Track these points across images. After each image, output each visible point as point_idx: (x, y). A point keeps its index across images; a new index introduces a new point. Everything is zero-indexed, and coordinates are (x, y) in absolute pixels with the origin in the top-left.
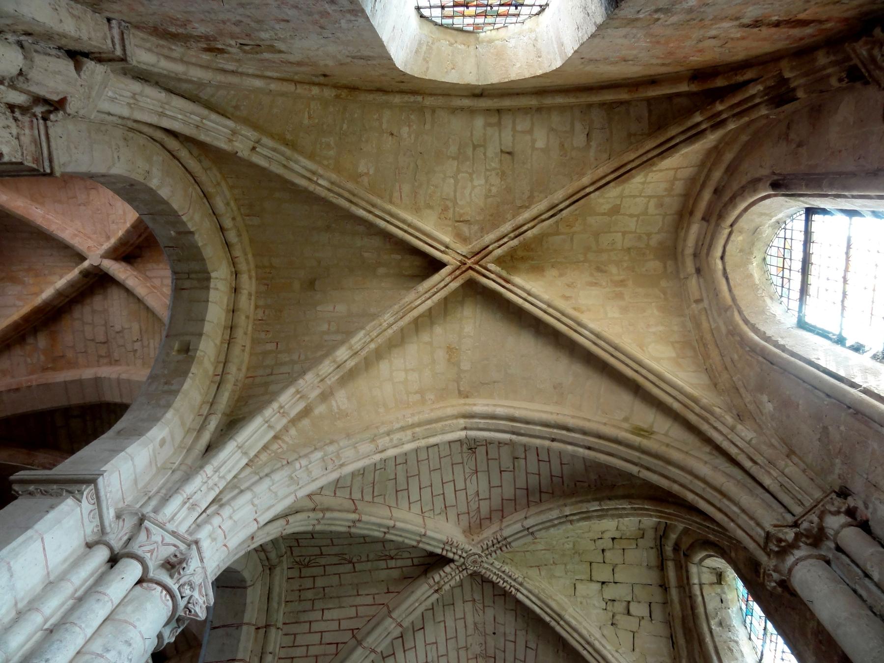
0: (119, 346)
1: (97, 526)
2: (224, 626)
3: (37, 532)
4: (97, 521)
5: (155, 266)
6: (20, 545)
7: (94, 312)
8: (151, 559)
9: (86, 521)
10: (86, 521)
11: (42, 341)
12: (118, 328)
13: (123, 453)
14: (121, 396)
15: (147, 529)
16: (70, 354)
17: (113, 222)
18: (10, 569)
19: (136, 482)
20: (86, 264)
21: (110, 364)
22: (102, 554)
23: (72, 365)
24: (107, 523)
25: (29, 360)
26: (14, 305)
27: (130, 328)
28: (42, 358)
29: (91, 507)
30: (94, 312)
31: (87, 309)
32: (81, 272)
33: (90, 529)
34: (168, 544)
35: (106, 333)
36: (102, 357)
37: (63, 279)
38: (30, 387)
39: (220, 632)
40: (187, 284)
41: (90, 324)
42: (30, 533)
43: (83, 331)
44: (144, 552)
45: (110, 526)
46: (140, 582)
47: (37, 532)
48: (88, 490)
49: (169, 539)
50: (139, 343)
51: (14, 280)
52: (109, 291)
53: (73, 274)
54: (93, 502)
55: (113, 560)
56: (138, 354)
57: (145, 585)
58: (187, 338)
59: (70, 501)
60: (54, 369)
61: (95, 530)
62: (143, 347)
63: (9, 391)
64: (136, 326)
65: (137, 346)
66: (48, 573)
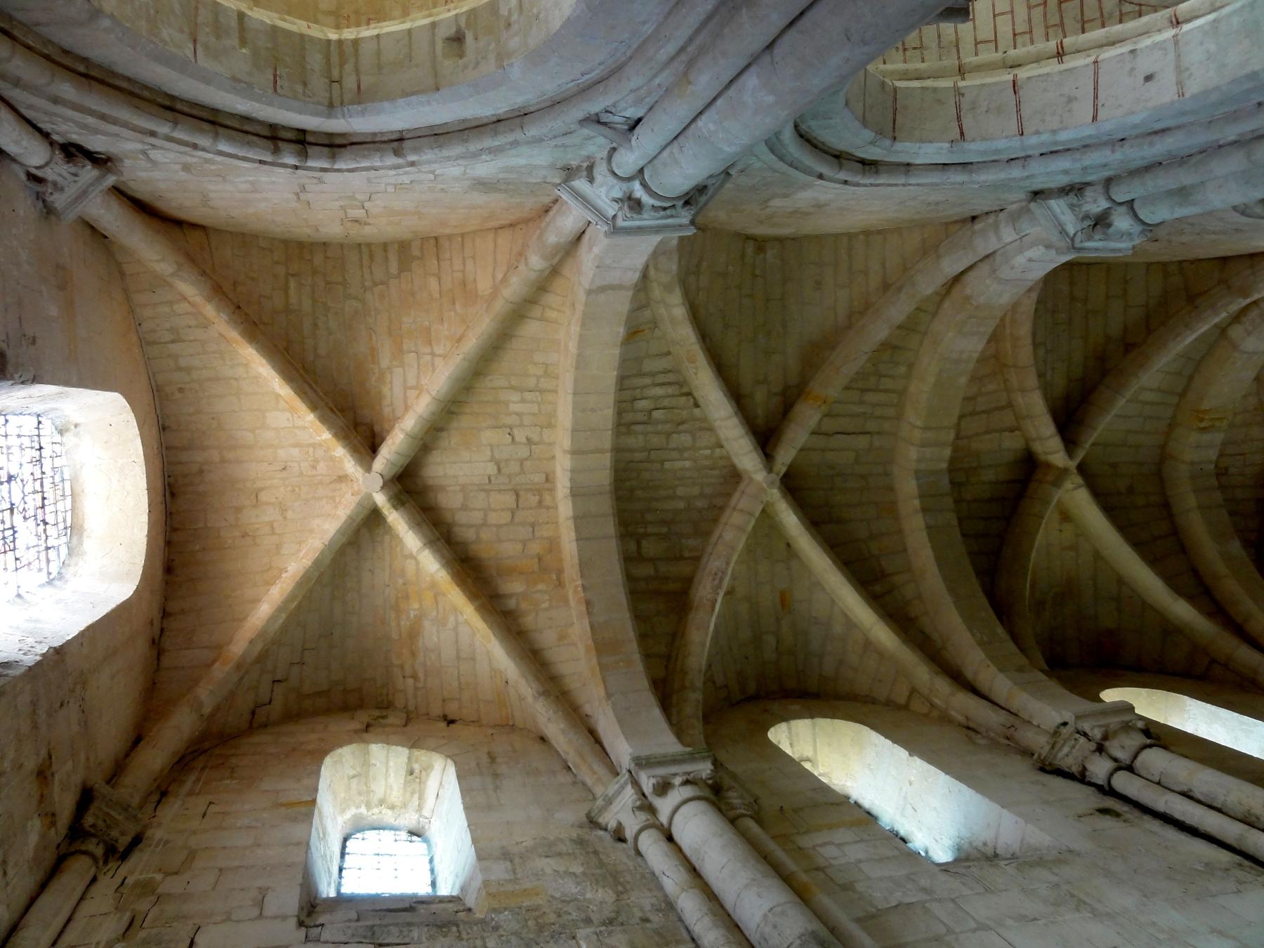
0: (522, 472)
2: (959, 118)
5: (386, 402)
7: (464, 508)
11: (513, 587)
12: (491, 469)
14: (601, 451)
16: (535, 548)
17: (314, 467)
20: (381, 499)
21: (552, 490)
23: (553, 545)
25: (543, 606)
26: (455, 629)
27: (491, 446)
28: (541, 587)
30: (464, 508)
31: (462, 518)
32: (395, 507)
35: (500, 491)
36: (540, 502)
37: (405, 532)
38: (583, 586)
39: (967, 122)
40: (350, 82)
41: (486, 516)
43: (499, 526)
50: (516, 432)
51: (414, 634)
52: (431, 482)
53: (396, 520)
56: (535, 438)
58: (439, 45)
60: (560, 572)
62: (521, 425)
63: (589, 613)
64: (488, 436)
65: (520, 436)
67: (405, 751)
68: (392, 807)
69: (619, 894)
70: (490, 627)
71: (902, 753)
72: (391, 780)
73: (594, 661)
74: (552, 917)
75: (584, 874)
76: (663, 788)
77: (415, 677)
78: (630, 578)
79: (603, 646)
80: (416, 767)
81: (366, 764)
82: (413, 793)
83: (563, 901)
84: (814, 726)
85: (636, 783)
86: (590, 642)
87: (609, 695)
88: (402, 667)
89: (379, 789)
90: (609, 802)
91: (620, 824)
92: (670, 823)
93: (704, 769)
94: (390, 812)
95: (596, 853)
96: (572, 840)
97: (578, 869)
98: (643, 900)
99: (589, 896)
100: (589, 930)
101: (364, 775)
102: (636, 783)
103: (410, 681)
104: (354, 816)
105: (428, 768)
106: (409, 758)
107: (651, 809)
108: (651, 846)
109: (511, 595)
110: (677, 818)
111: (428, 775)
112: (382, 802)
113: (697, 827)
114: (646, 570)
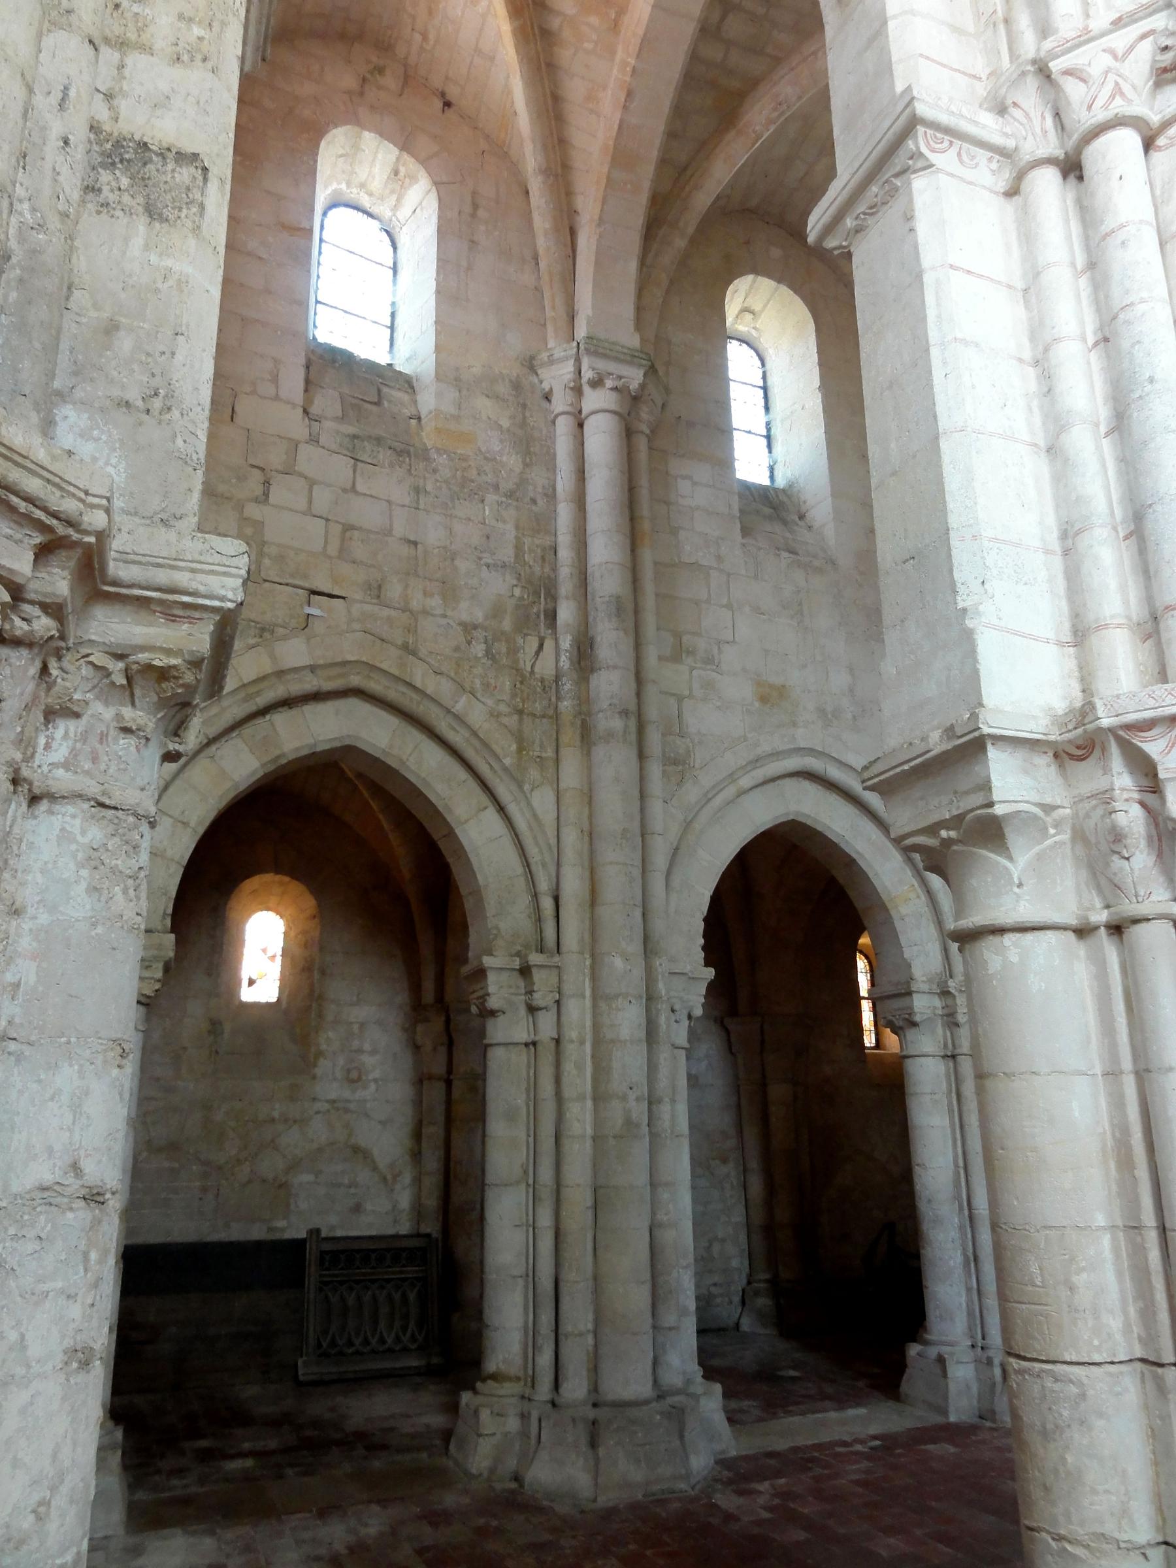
1: (990, 159)
3: (933, 268)
4: (982, 155)
6: (938, 305)
8: (1130, 101)
9: (968, 174)
10: (968, 174)
13: (891, 25)
15: (1068, 72)
18: (965, 342)
19: (957, 30)
22: (1047, 185)
24: (997, 140)
25: (586, 45)
28: (594, 20)
29: (953, 152)
33: (988, 175)
34: (1131, 48)
38: (634, 70)
42: (928, 279)
44: (1105, 107)
45: (1006, 135)
46: (1148, 145)
47: (933, 268)
48: (922, 140)
49: (1121, 40)
54: (946, 144)
55: (1072, 168)
57: (1161, 141)
59: (919, 184)
60: (622, 11)
61: (994, 166)
63: (625, 107)
66: (1009, 287)
67: (396, 151)
68: (371, 194)
69: (526, 465)
70: (521, 62)
71: (817, 382)
72: (376, 170)
73: (605, 170)
74: (473, 474)
75: (508, 430)
76: (597, 383)
77: (425, 38)
78: (694, 57)
79: (622, 156)
80: (402, 170)
81: (356, 148)
82: (393, 192)
83: (486, 458)
84: (776, 289)
85: (578, 360)
86: (611, 143)
87: (601, 221)
88: (414, 18)
89: (362, 174)
90: (551, 361)
91: (551, 389)
92: (586, 418)
93: (635, 377)
94: (366, 197)
95: (524, 406)
96: (511, 381)
97: (505, 423)
98: (538, 477)
99: (504, 459)
100: (496, 497)
101: (352, 154)
102: (578, 360)
103: (418, 37)
104: (335, 191)
105: (413, 179)
106: (398, 159)
107: (578, 391)
108: (564, 426)
109: (559, 13)
110: (593, 417)
111: (411, 185)
112: (362, 186)
113: (601, 440)
114: (714, 52)
